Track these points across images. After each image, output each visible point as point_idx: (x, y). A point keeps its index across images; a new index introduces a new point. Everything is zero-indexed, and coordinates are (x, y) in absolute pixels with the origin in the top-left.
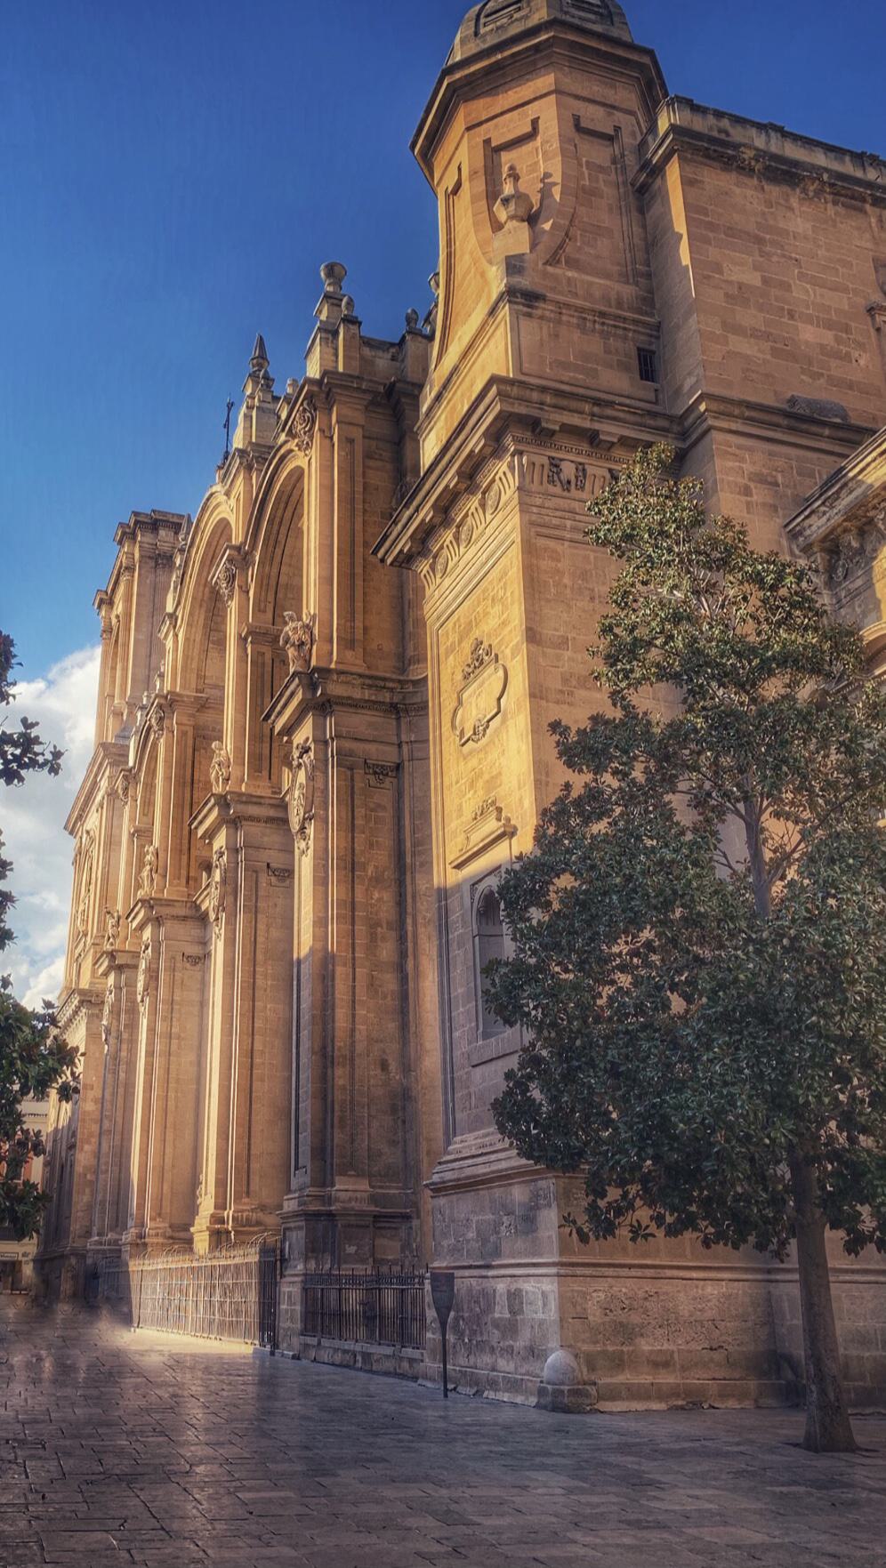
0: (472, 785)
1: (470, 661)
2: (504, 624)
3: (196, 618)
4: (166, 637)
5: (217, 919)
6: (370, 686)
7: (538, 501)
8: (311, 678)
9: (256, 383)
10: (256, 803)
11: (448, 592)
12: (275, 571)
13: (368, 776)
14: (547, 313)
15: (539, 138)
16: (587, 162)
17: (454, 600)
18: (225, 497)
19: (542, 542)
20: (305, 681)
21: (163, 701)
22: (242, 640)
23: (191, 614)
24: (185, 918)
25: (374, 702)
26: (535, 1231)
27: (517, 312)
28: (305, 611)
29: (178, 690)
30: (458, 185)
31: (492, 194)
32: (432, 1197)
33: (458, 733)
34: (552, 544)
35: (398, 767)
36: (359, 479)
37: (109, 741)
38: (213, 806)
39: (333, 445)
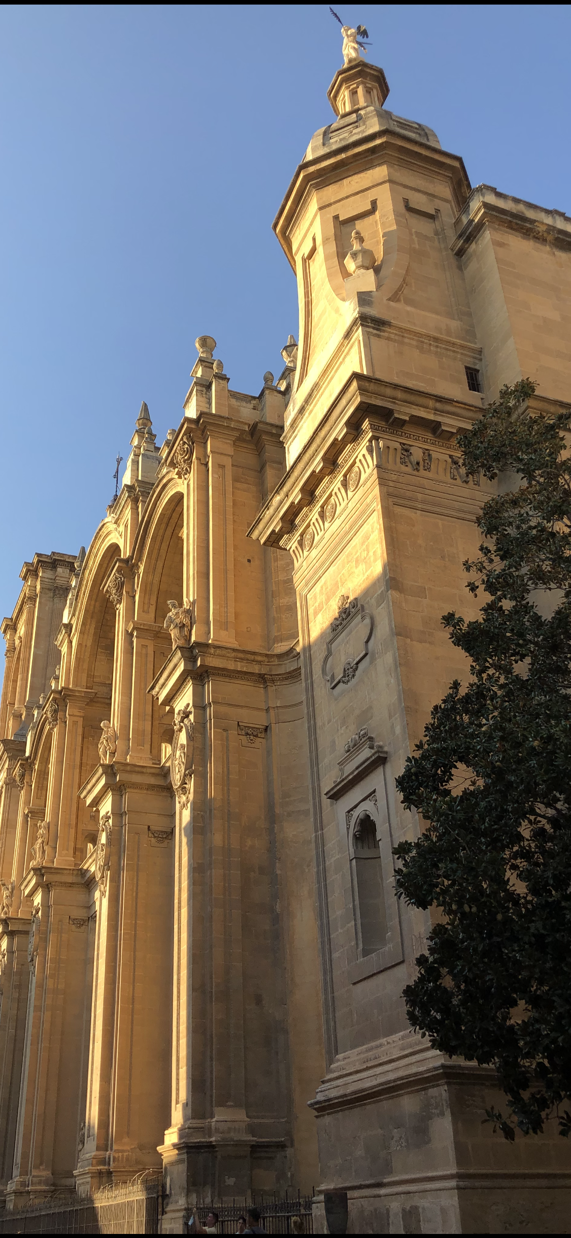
3: (88, 627)
5: (102, 877)
7: (394, 477)
10: (138, 772)
11: (315, 561)
12: (157, 579)
13: (241, 737)
14: (392, 336)
15: (377, 213)
16: (416, 232)
17: (320, 567)
18: (115, 526)
19: (398, 510)
20: (187, 654)
21: (57, 696)
22: (129, 635)
23: (84, 624)
24: (71, 885)
25: (246, 673)
26: (429, 1141)
27: (368, 333)
28: (185, 599)
30: (313, 250)
31: (341, 256)
32: (317, 1117)
33: (328, 678)
35: (266, 729)
36: (229, 496)
39: (208, 470)
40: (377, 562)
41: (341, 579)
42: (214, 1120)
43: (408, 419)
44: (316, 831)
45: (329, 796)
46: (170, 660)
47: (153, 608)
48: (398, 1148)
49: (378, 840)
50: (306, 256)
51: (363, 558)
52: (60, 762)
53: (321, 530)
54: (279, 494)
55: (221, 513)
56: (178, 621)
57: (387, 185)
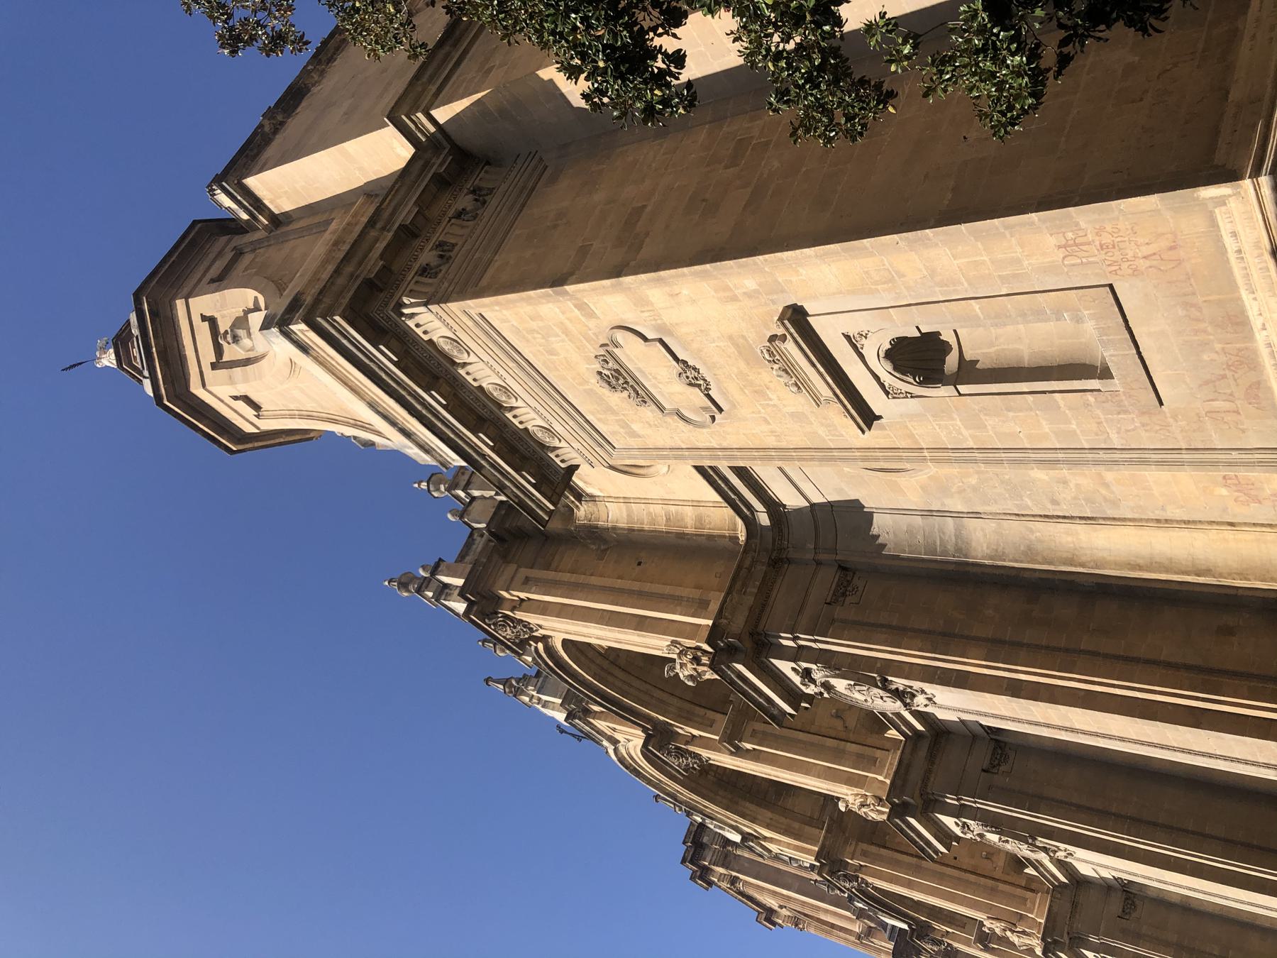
0: (760, 393)
1: (625, 394)
2: (566, 332)
3: (748, 812)
4: (769, 851)
7: (446, 284)
8: (722, 649)
9: (523, 693)
12: (675, 701)
19: (484, 282)
21: (827, 868)
22: (739, 752)
29: (817, 849)
30: (247, 400)
34: (490, 271)
35: (843, 568)
37: (892, 947)
40: (541, 314)
41: (580, 384)
43: (382, 263)
44: (924, 459)
47: (711, 714)
49: (919, 335)
50: (256, 414)
51: (543, 341)
52: (909, 885)
56: (689, 666)
57: (190, 300)
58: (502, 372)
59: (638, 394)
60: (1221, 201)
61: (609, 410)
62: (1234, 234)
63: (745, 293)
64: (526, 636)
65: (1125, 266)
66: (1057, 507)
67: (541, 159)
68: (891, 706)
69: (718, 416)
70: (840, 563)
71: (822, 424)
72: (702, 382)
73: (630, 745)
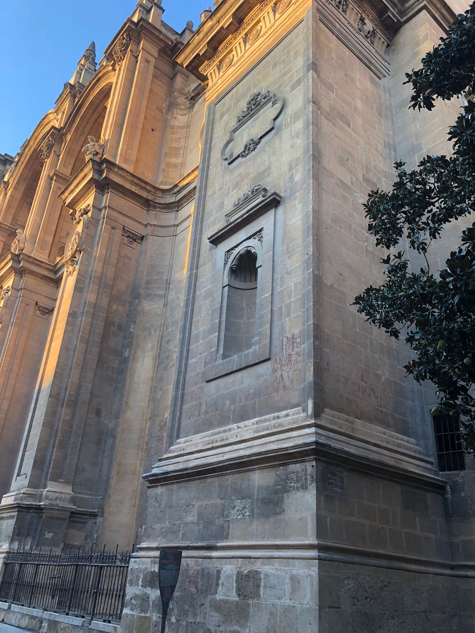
1: (245, 110)
6: (136, 185)
11: (230, 77)
13: (124, 237)
19: (321, 25)
20: (96, 167)
26: (282, 511)
28: (102, 137)
35: (142, 238)
38: (10, 260)
39: (137, 62)
42: (46, 490)
45: (211, 240)
46: (82, 170)
48: (239, 517)
49: (257, 267)
51: (282, 60)
53: (241, 52)
54: (212, 19)
55: (140, 89)
58: (267, 35)
59: (244, 117)
60: (305, 410)
61: (238, 101)
62: (287, 415)
63: (293, 175)
64: (116, 59)
65: (279, 366)
66: (166, 343)
67: (385, 77)
68: (68, 254)
69: (227, 162)
70: (146, 237)
71: (215, 219)
72: (247, 153)
73: (55, 121)
